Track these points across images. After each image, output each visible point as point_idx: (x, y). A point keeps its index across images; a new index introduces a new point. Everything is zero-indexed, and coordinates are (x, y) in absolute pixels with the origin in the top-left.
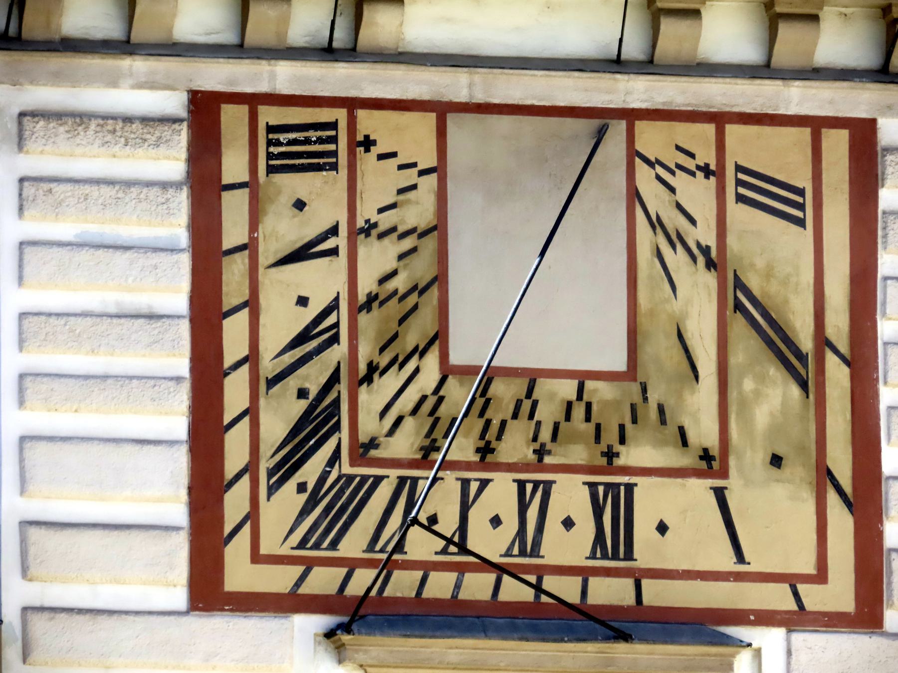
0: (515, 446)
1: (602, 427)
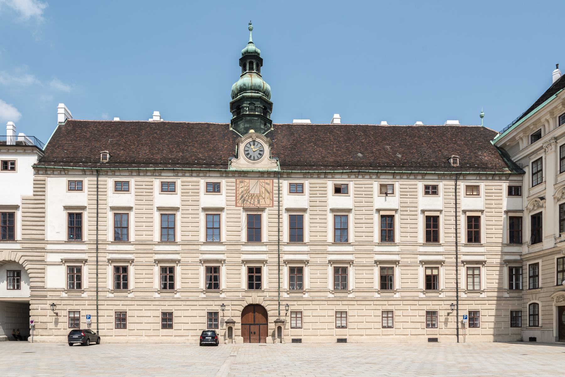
1: (258, 196)
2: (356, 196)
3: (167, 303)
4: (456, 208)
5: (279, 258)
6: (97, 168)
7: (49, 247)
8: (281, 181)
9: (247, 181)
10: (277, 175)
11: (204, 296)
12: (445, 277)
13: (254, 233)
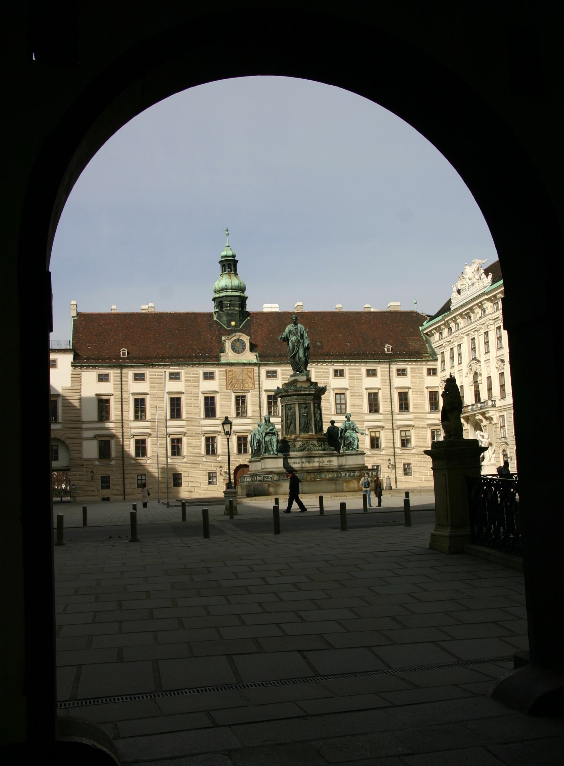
6: (121, 364)
7: (84, 426)
10: (255, 364)
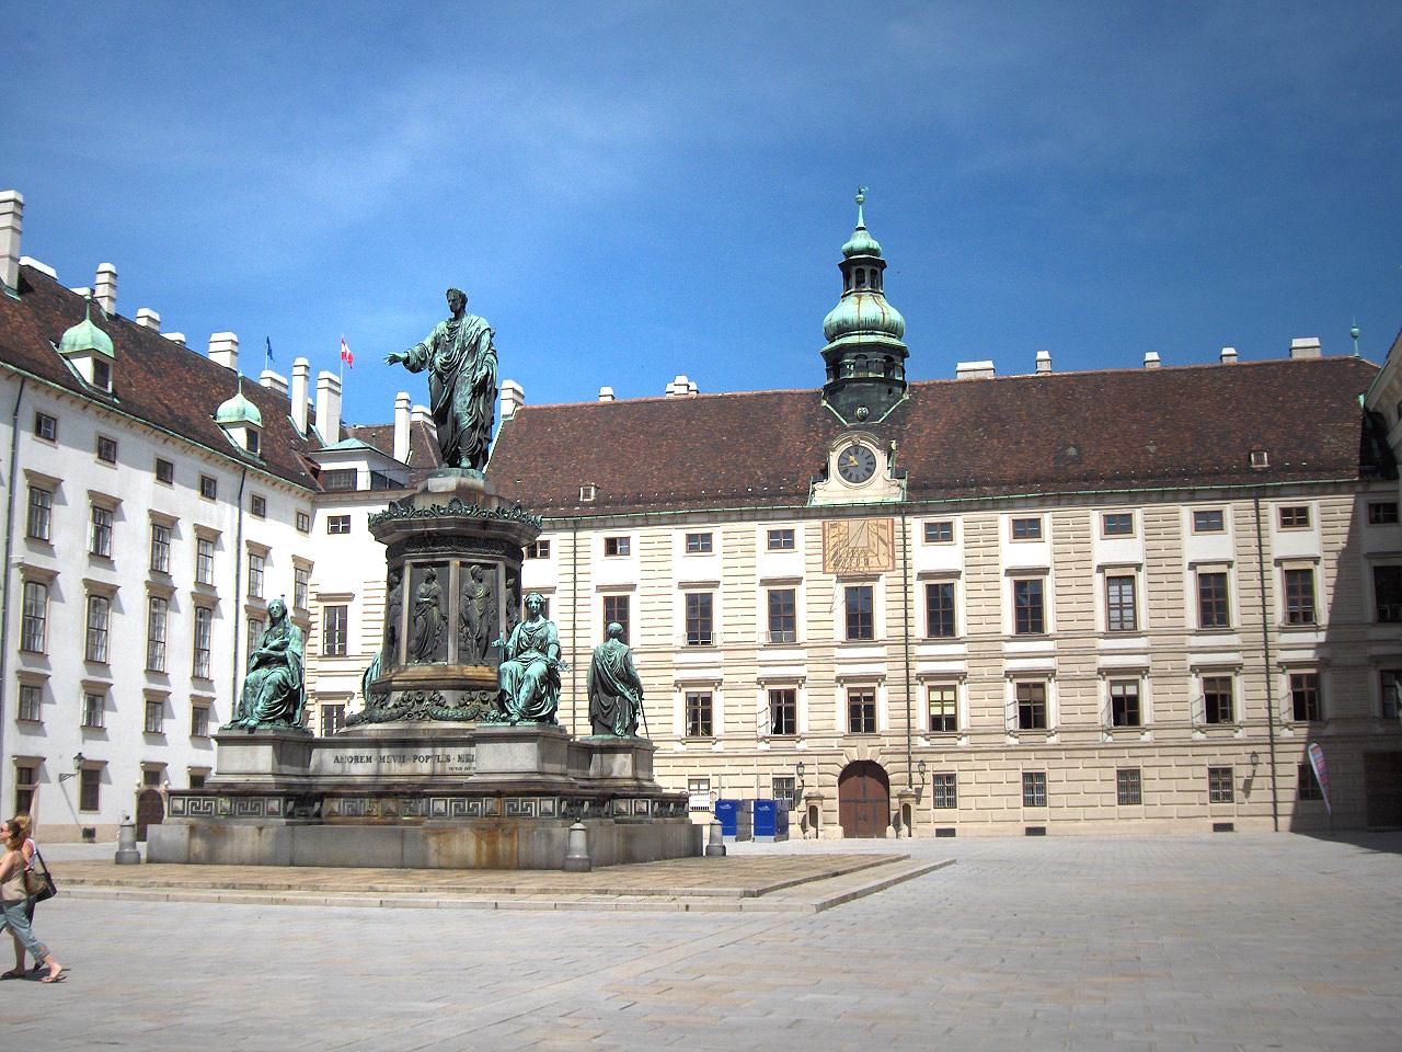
0: (856, 555)
1: (866, 551)
2: (1057, 540)
3: (697, 762)
4: (1261, 554)
5: (907, 670)
8: (907, 520)
9: (845, 524)
11: (767, 747)
12: (1244, 697)
13: (859, 624)
